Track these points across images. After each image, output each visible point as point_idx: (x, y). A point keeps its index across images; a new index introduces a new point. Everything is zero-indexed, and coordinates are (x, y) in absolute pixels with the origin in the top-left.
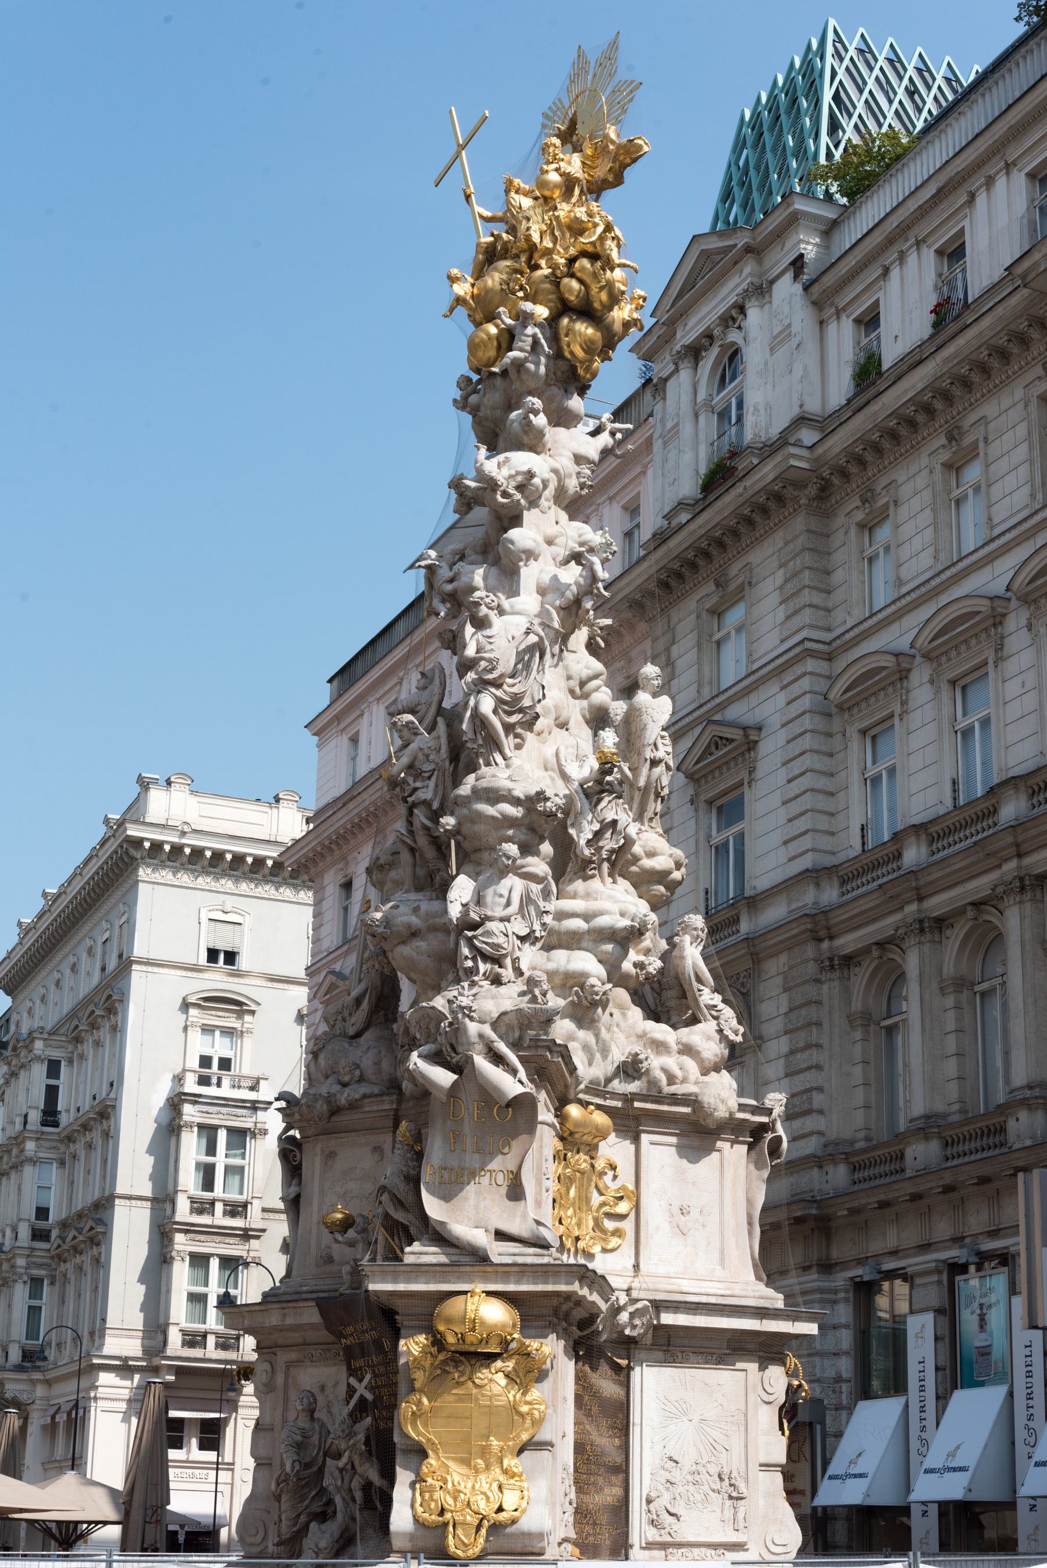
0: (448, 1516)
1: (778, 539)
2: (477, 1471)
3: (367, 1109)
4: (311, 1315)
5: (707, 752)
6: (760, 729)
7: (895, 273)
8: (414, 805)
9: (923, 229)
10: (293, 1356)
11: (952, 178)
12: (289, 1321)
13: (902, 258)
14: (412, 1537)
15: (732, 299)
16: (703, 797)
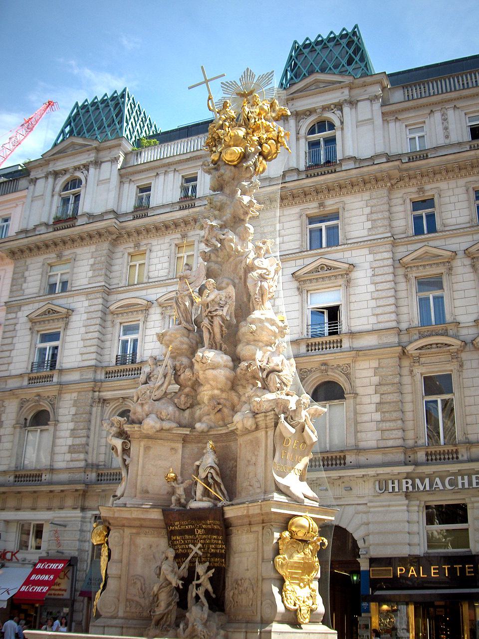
0: (297, 607)
1: (93, 248)
2: (301, 587)
3: (175, 432)
4: (156, 515)
5: (44, 313)
6: (73, 311)
7: (161, 177)
8: (216, 315)
9: (179, 168)
10: (134, 531)
11: (197, 156)
12: (142, 517)
13: (166, 173)
14: (283, 615)
15: (84, 162)
16: (36, 329)
